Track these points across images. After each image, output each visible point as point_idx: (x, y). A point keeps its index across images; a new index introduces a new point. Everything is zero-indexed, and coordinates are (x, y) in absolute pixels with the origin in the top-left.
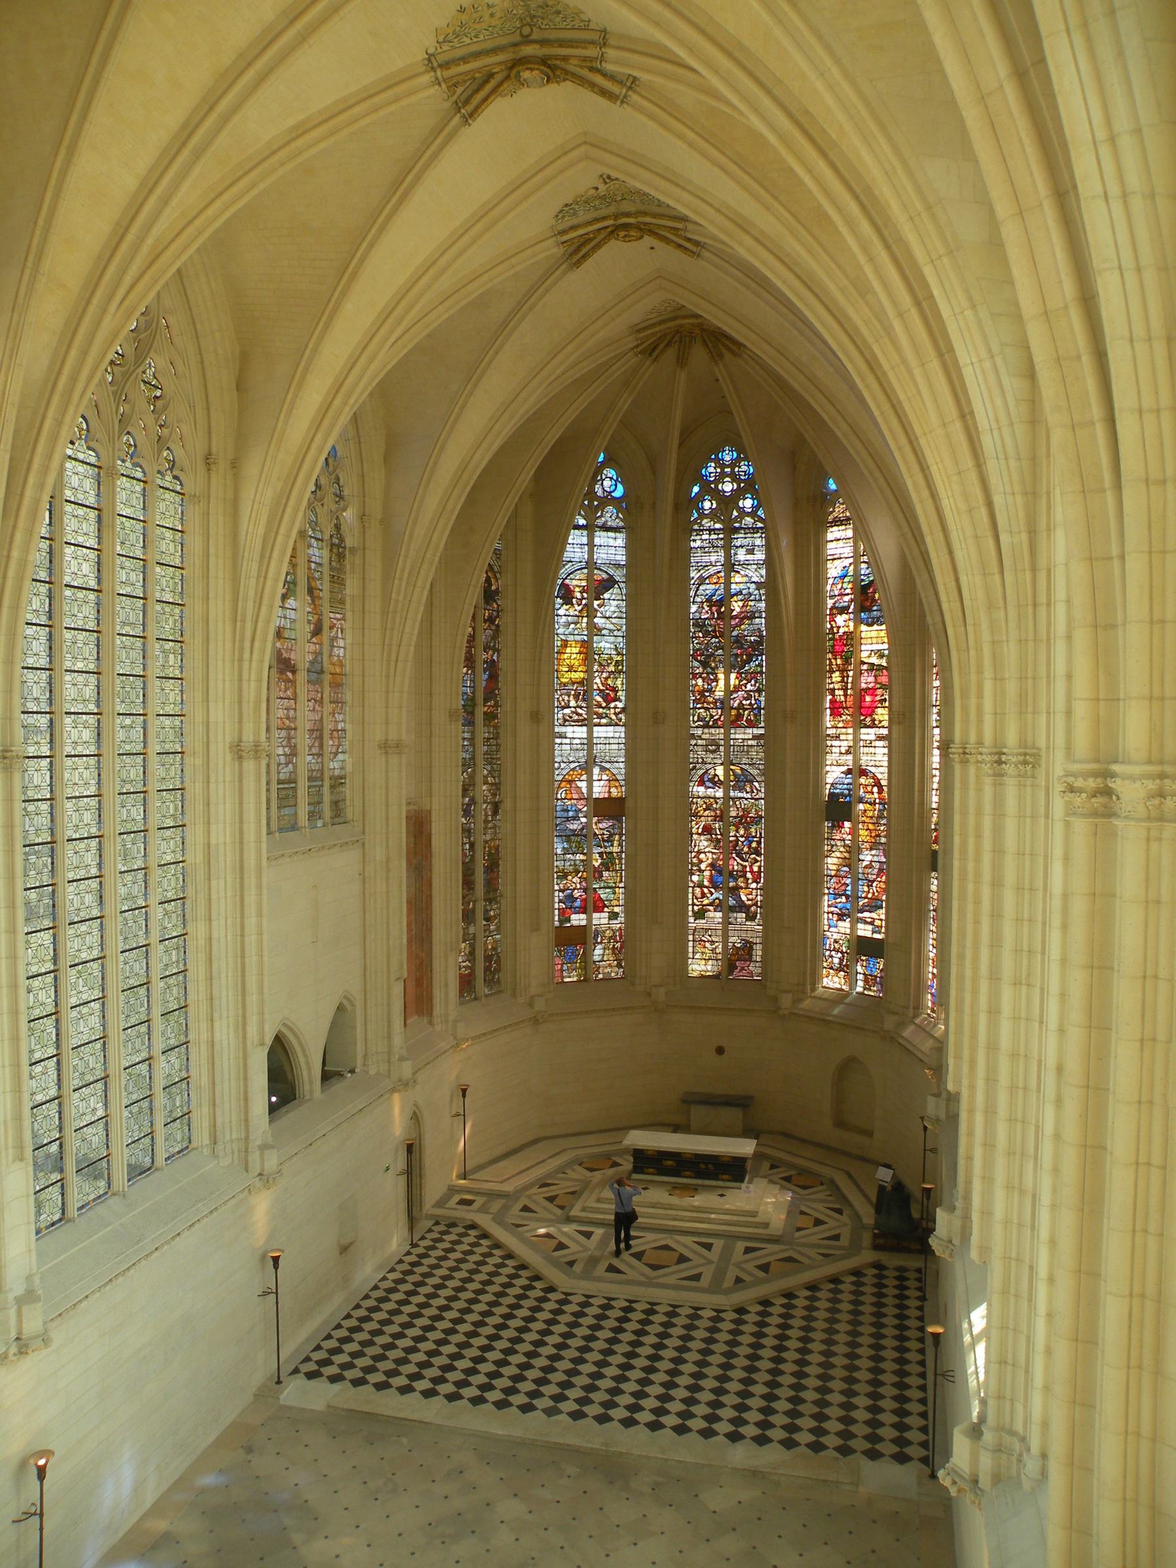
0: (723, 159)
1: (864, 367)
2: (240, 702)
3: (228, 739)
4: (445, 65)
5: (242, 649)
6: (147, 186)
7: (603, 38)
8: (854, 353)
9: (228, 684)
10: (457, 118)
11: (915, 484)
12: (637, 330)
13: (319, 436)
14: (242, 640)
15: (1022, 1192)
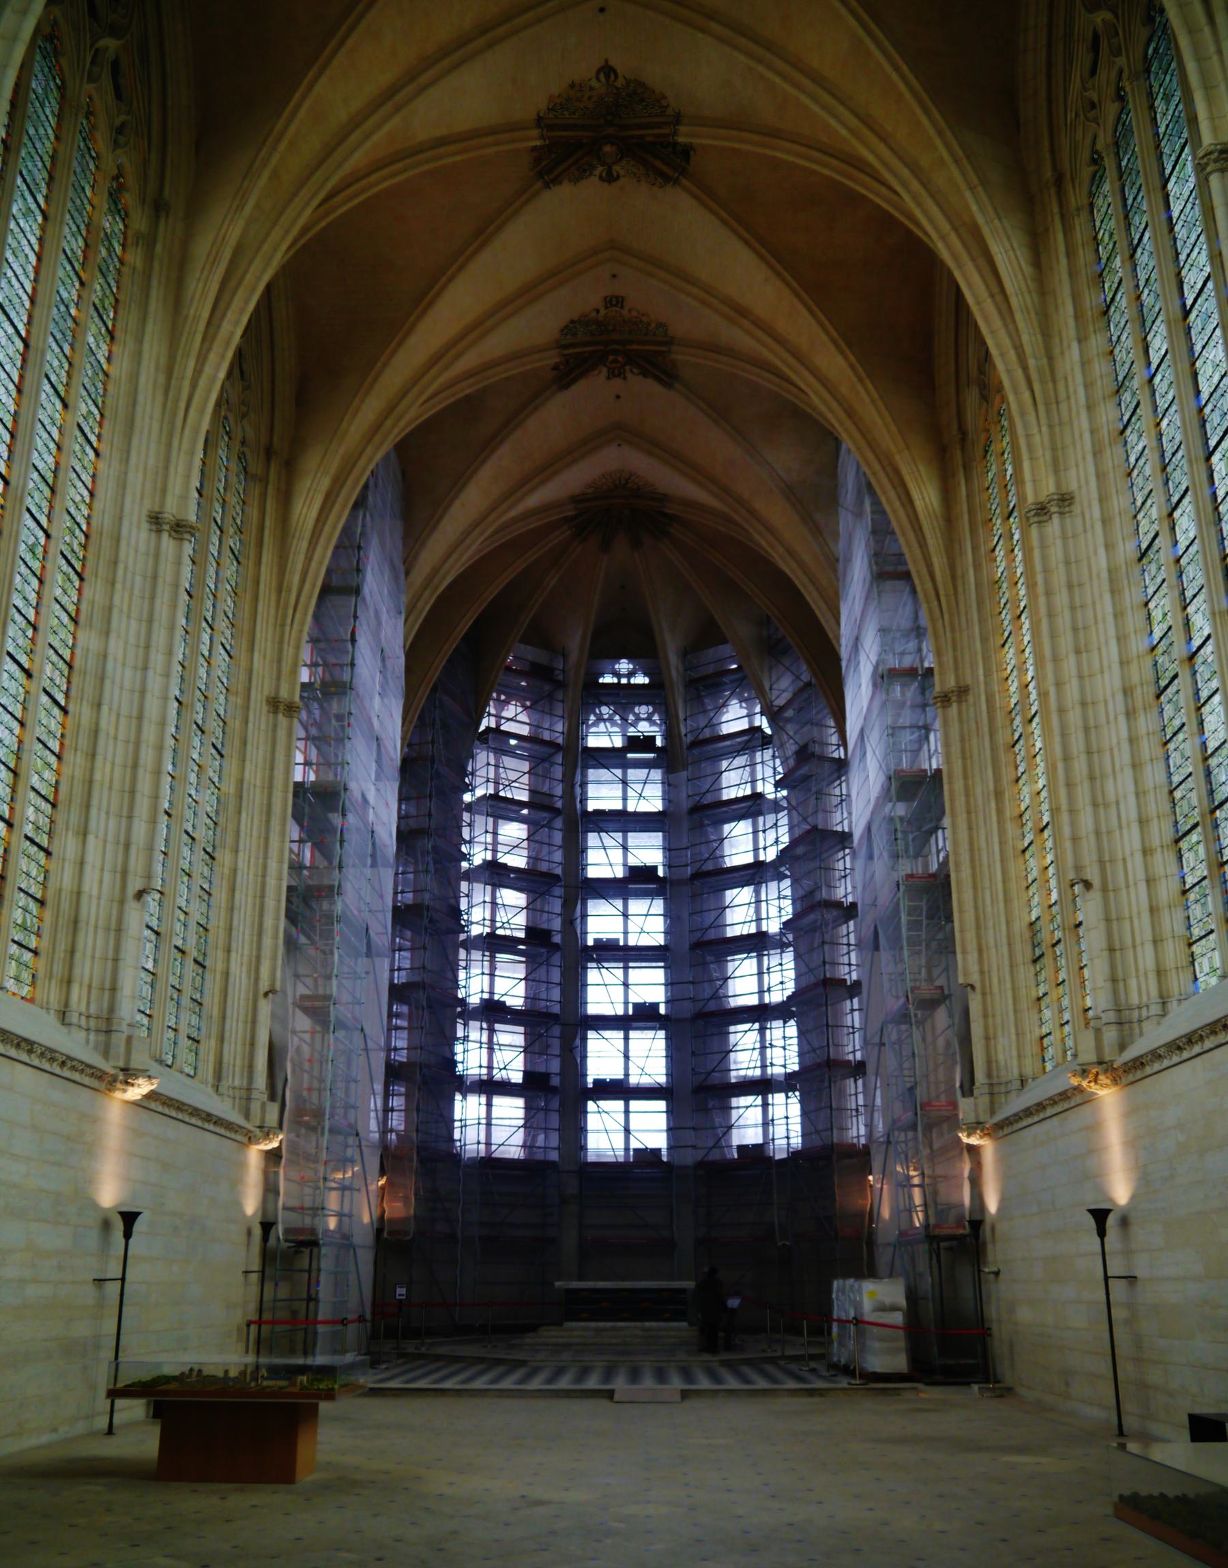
0: (747, 235)
1: (842, 415)
2: (279, 661)
3: (266, 693)
4: (551, 128)
5: (285, 616)
6: (355, 123)
7: (678, 119)
8: (835, 405)
9: (269, 643)
10: (539, 184)
11: (888, 500)
12: (575, 499)
13: (369, 450)
14: (286, 607)
15: (1106, 805)
